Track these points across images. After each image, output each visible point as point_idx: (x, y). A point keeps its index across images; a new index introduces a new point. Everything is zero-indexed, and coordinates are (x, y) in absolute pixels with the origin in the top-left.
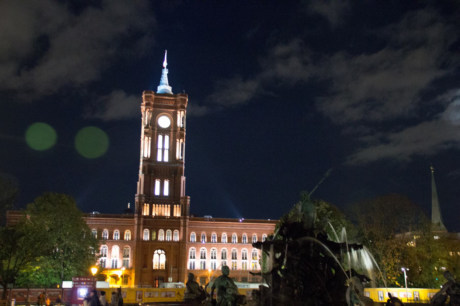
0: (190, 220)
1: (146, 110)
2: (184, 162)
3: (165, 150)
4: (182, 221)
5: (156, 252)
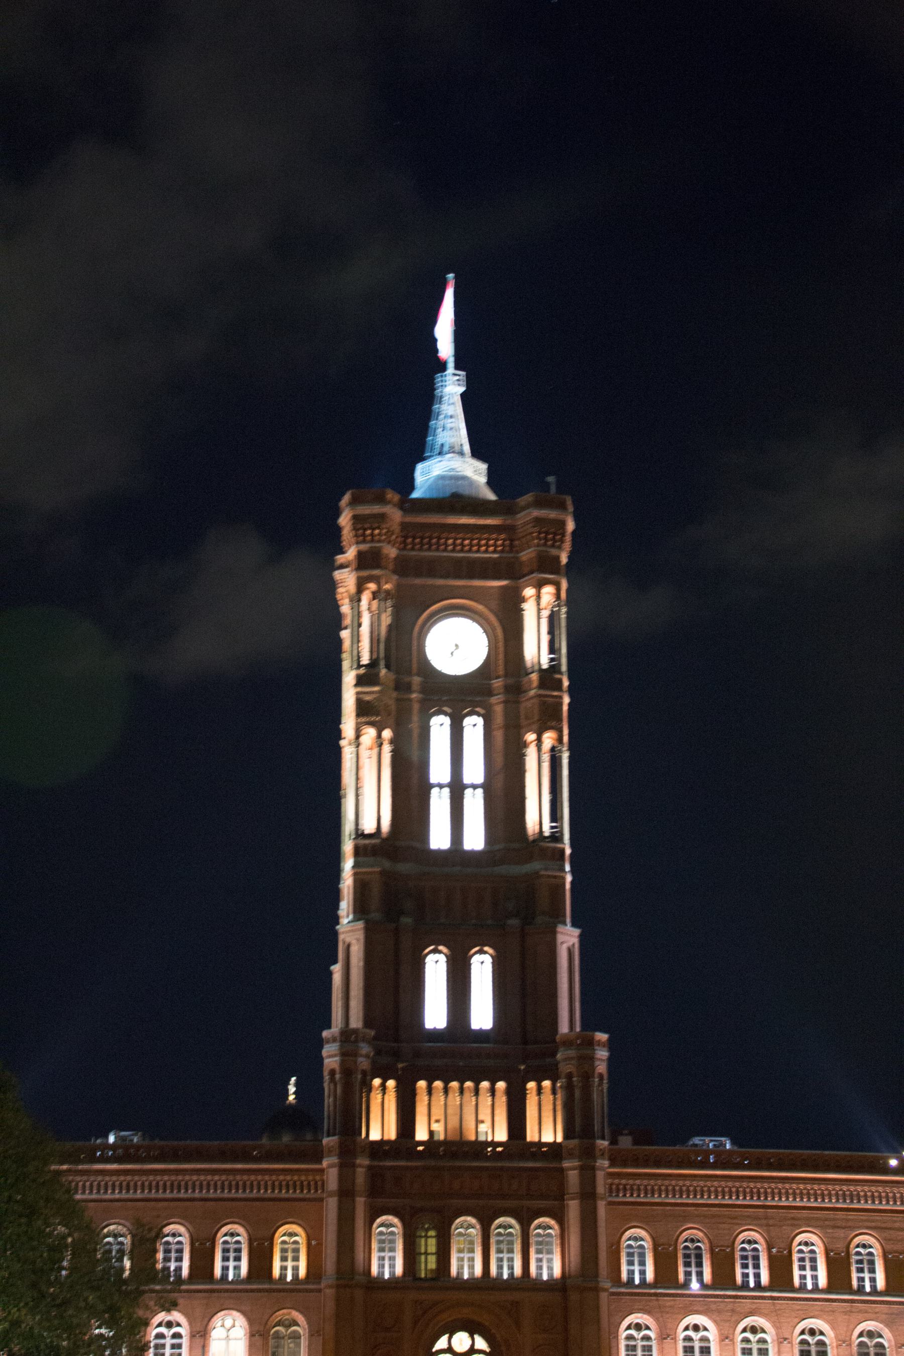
0: (613, 1164)
1: (360, 589)
2: (568, 851)
3: (468, 792)
4: (571, 1168)
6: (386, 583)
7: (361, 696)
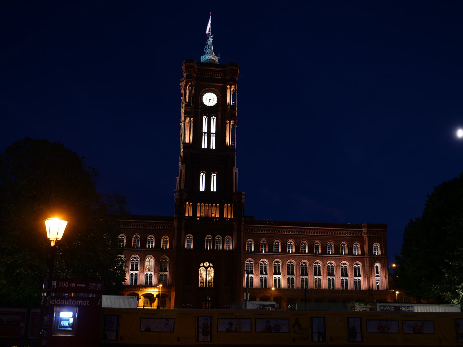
1: (187, 84)
5: (202, 264)
6: (193, 83)
7: (186, 110)
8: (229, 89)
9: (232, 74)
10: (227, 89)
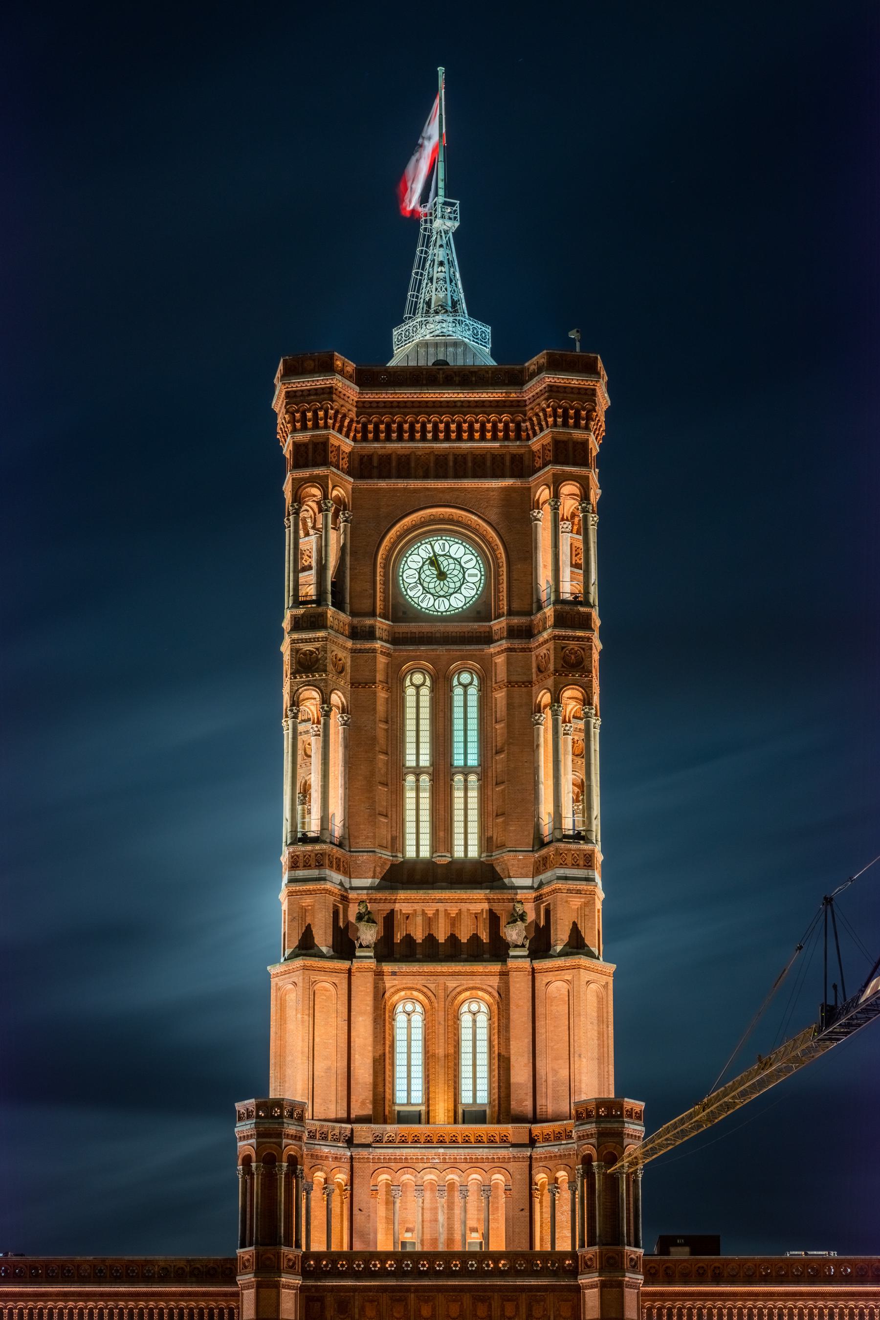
0: (651, 1277)
2: (599, 857)
8: (546, 506)
9: (560, 420)
10: (537, 506)
